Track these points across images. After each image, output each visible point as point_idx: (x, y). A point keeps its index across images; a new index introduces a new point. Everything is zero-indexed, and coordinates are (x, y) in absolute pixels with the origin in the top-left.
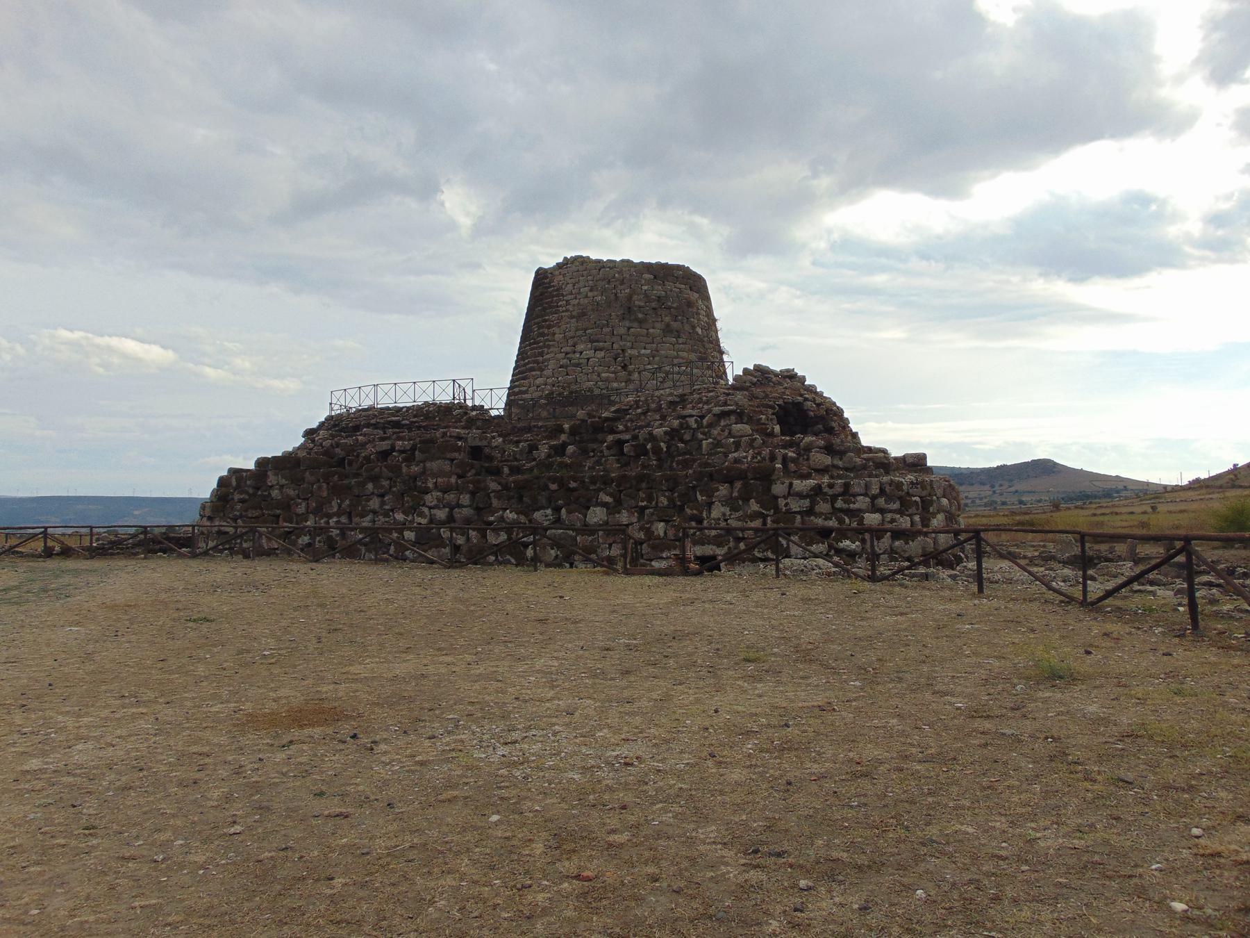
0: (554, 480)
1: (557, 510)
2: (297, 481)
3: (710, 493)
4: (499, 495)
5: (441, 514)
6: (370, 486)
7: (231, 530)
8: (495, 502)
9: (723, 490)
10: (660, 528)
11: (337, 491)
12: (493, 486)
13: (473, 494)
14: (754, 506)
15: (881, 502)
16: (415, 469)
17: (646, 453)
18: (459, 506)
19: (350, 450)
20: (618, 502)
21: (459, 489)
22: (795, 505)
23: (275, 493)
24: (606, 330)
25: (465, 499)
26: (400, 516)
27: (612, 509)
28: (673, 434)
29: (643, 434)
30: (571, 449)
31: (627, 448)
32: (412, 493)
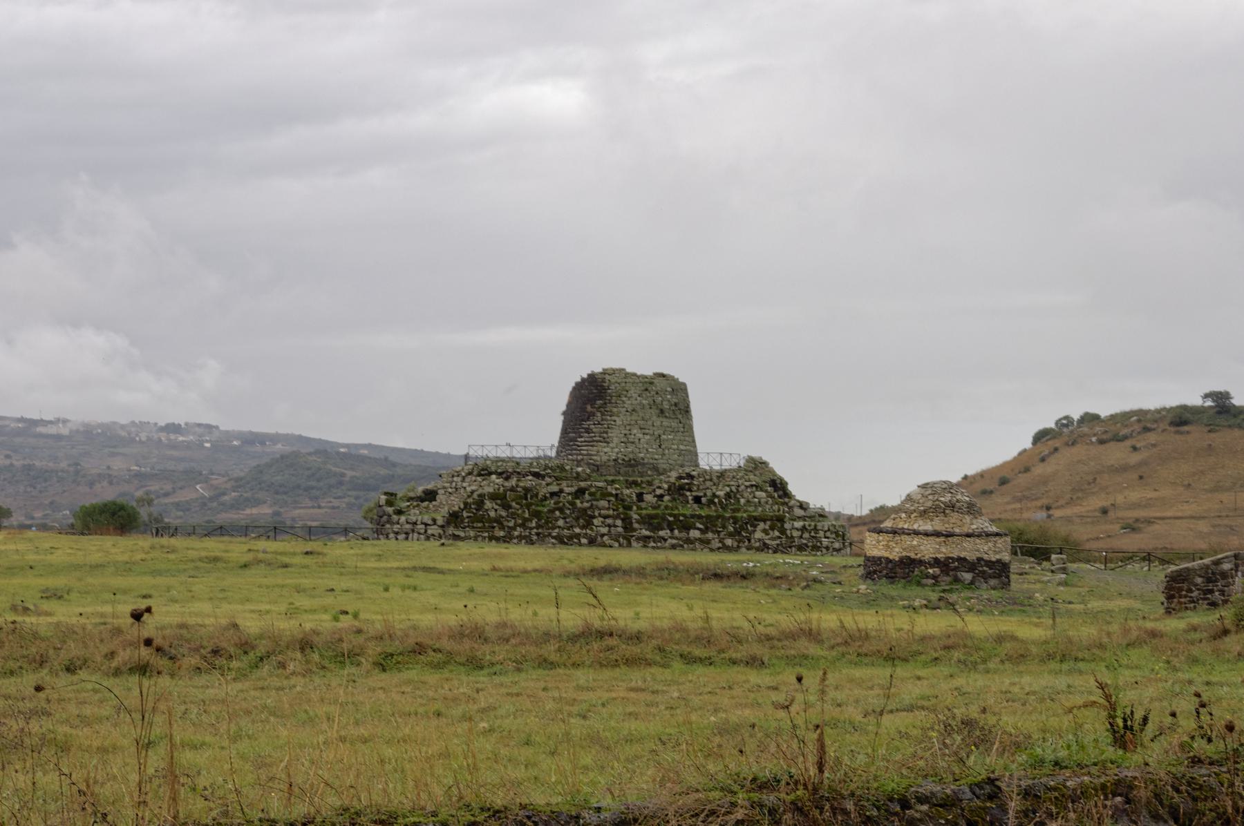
0: (670, 515)
1: (672, 530)
2: (506, 507)
3: (755, 526)
4: (638, 522)
5: (604, 530)
6: (557, 513)
7: (462, 534)
8: (636, 526)
9: (762, 525)
10: (729, 542)
11: (537, 514)
12: (636, 516)
13: (623, 520)
14: (777, 533)
15: (828, 534)
16: (586, 505)
17: (715, 504)
18: (616, 526)
19: (527, 490)
20: (707, 528)
21: (615, 517)
22: (796, 534)
23: (492, 514)
24: (650, 423)
25: (619, 522)
26: (577, 530)
27: (703, 532)
28: (728, 496)
29: (709, 493)
30: (667, 498)
31: (704, 500)
32: (586, 518)
